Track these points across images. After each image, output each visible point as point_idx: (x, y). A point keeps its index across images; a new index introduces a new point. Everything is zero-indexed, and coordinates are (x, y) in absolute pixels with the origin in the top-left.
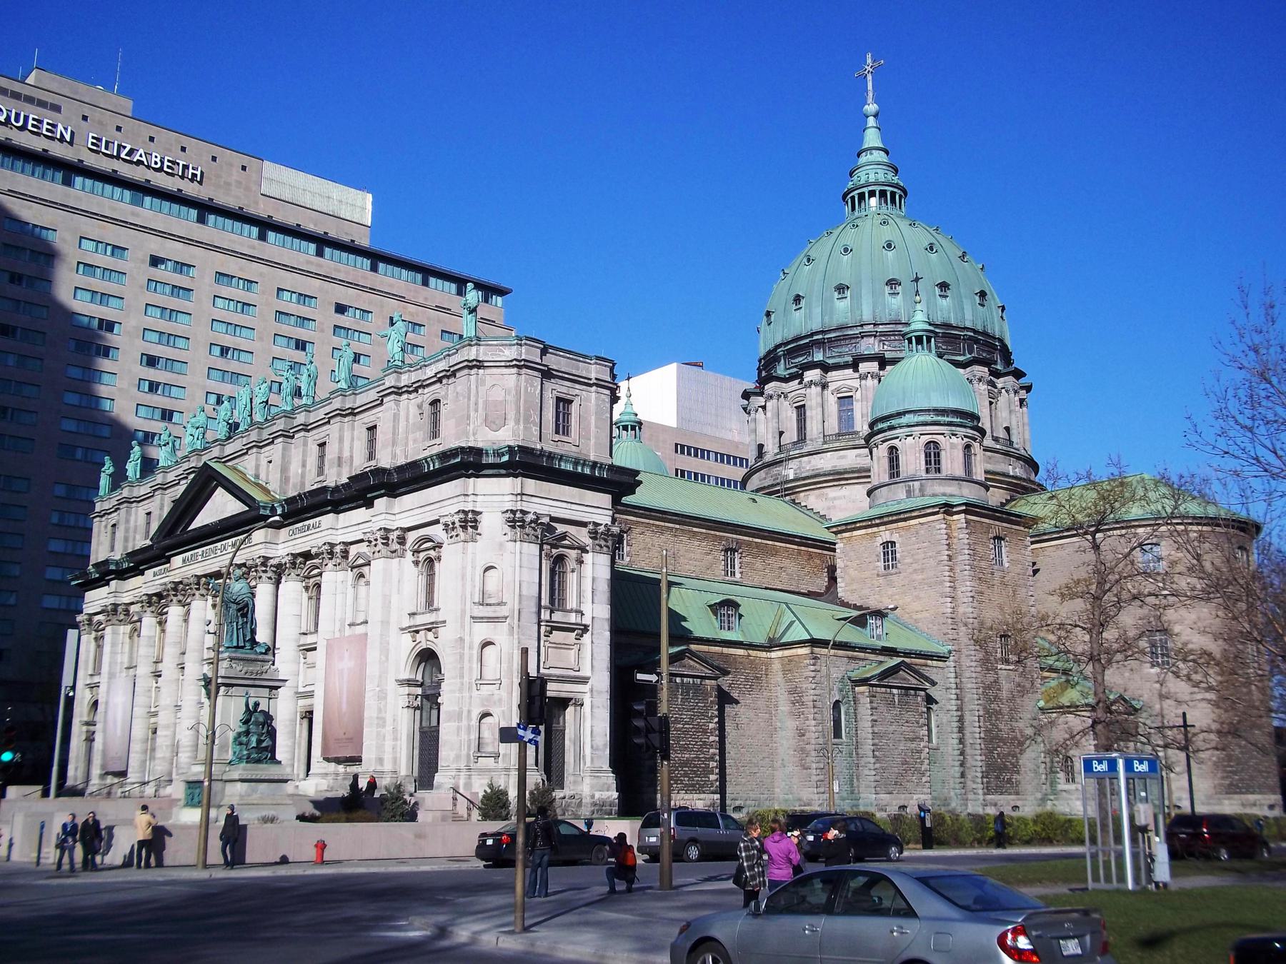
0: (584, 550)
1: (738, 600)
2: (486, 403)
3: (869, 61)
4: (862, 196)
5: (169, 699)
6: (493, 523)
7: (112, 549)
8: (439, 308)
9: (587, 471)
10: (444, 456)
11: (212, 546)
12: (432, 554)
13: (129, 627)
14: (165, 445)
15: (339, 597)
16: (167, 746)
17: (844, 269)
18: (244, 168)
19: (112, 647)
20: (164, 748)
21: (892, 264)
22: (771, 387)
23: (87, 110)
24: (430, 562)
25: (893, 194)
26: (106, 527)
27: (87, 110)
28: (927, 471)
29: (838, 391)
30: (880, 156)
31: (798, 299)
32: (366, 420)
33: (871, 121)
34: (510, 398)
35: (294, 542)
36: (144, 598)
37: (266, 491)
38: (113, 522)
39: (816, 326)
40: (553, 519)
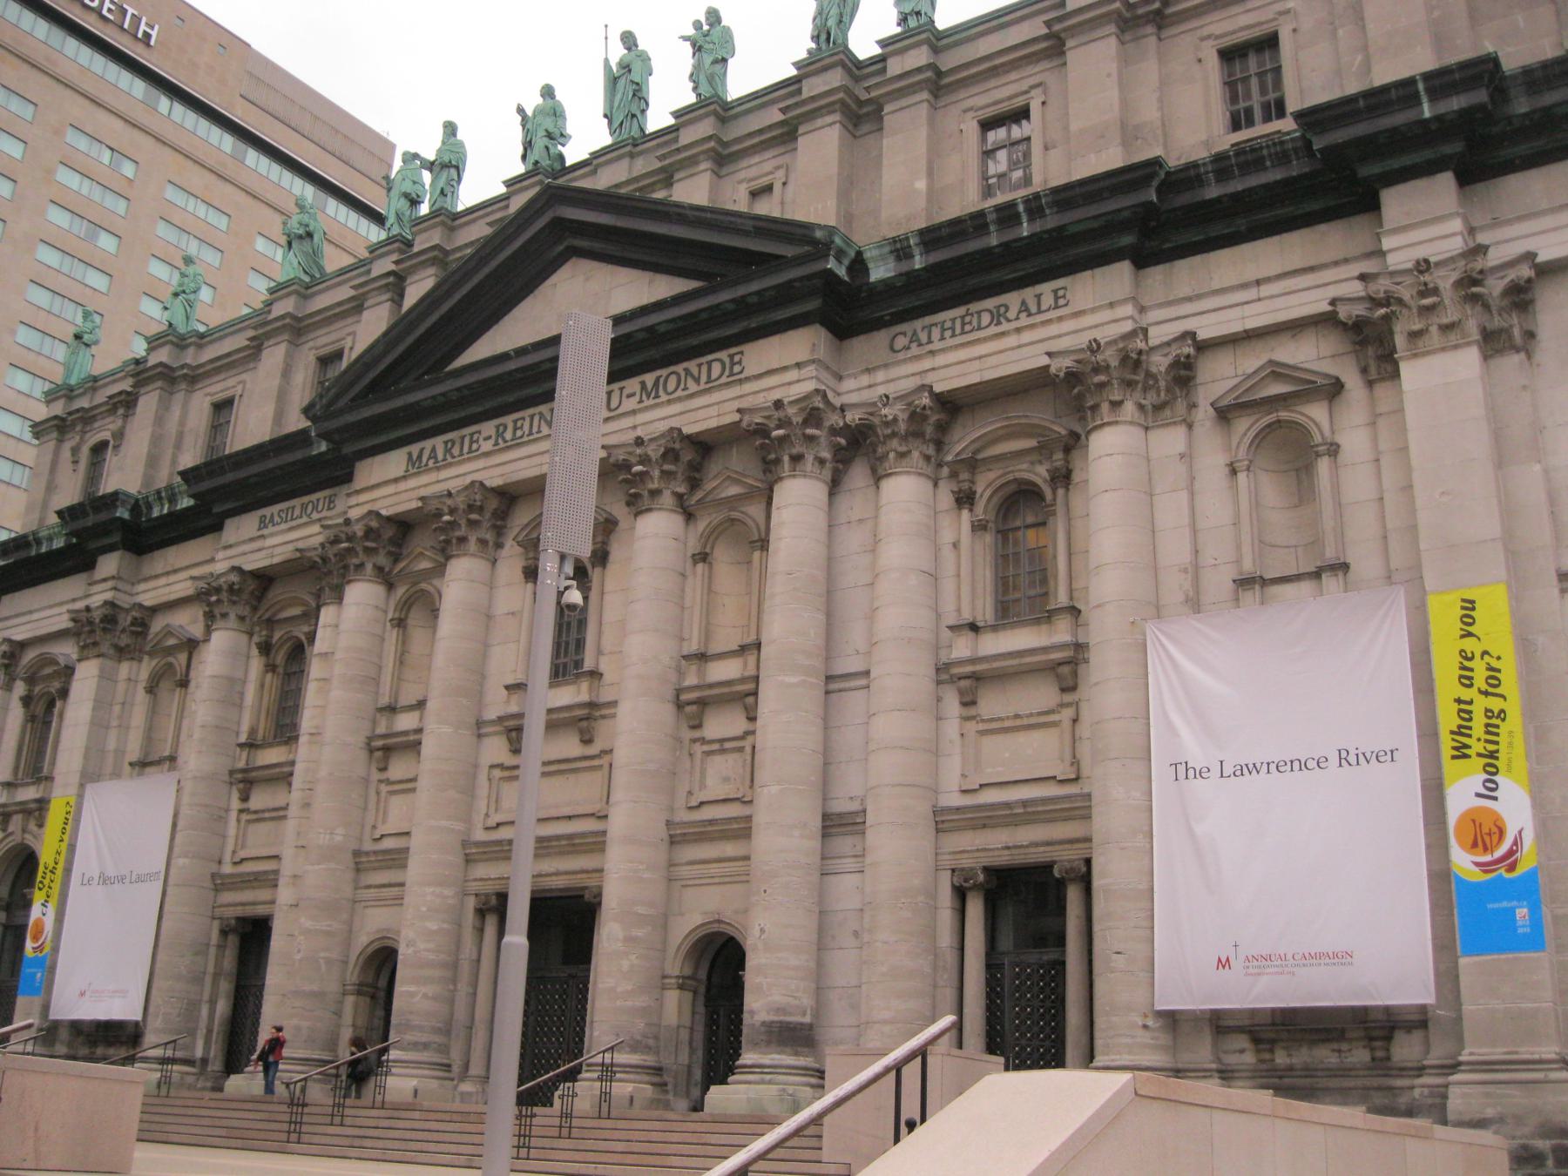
5: (340, 831)
13: (145, 669)
14: (300, 237)
15: (1171, 509)
16: (329, 962)
19: (94, 709)
20: (323, 968)
26: (75, 451)
32: (1218, 29)
35: (927, 364)
36: (234, 578)
38: (105, 435)
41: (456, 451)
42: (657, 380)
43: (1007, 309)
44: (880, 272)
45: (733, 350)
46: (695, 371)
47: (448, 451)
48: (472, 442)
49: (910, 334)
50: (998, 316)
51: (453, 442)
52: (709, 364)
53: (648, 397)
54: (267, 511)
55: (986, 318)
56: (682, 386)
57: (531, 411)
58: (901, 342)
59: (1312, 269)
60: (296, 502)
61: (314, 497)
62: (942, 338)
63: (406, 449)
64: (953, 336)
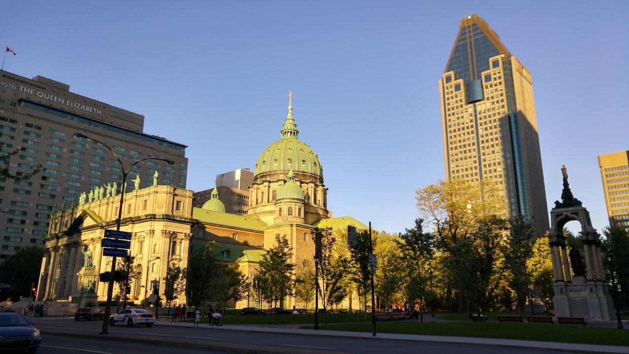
0: (183, 239)
1: (231, 250)
2: (158, 202)
3: (290, 93)
4: (285, 132)
6: (158, 233)
7: (55, 230)
8: (164, 152)
9: (184, 220)
10: (146, 216)
12: (142, 240)
17: (277, 154)
18: (104, 108)
21: (290, 154)
22: (255, 186)
23: (54, 89)
24: (142, 242)
25: (294, 133)
27: (54, 89)
28: (289, 215)
29: (273, 189)
30: (291, 121)
31: (264, 162)
33: (290, 110)
34: (165, 201)
37: (101, 218)
39: (268, 170)
40: (173, 232)
44: (104, 225)
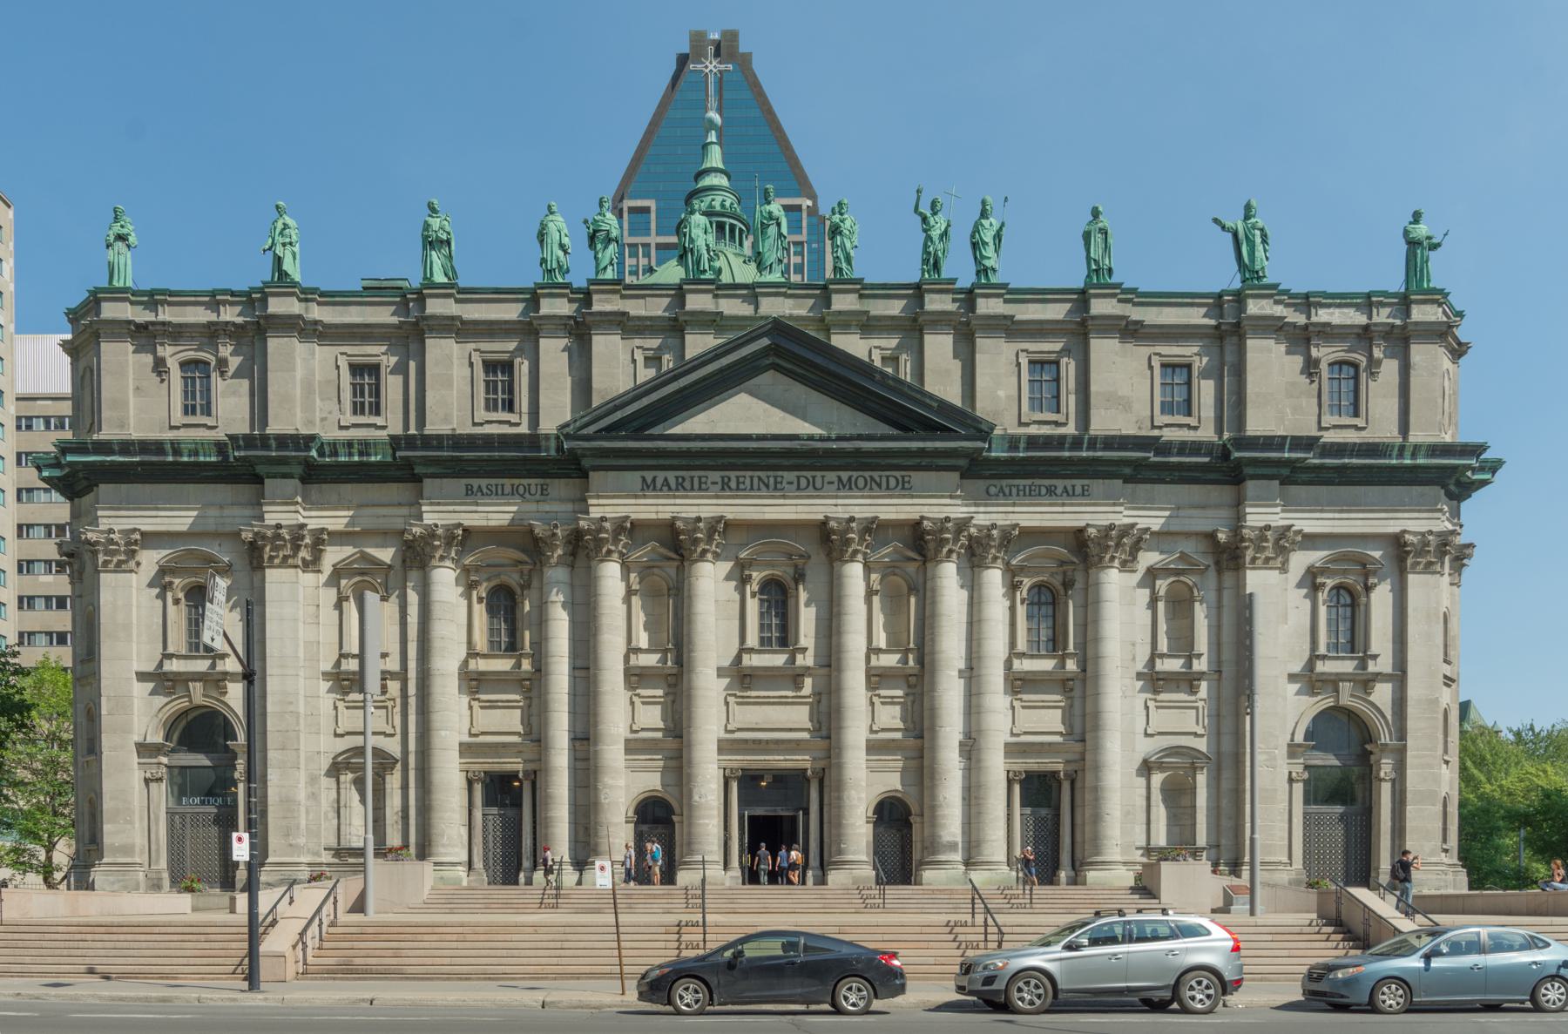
11: (762, 474)
41: (687, 484)
42: (850, 478)
43: (1056, 488)
45: (903, 473)
46: (878, 479)
47: (677, 484)
48: (700, 483)
49: (998, 488)
50: (1051, 491)
51: (684, 479)
52: (888, 477)
53: (844, 486)
54: (475, 482)
55: (1044, 491)
56: (868, 486)
57: (749, 473)
58: (993, 490)
59: (1203, 507)
60: (507, 482)
61: (525, 482)
62: (1018, 495)
63: (638, 474)
64: (1025, 495)
